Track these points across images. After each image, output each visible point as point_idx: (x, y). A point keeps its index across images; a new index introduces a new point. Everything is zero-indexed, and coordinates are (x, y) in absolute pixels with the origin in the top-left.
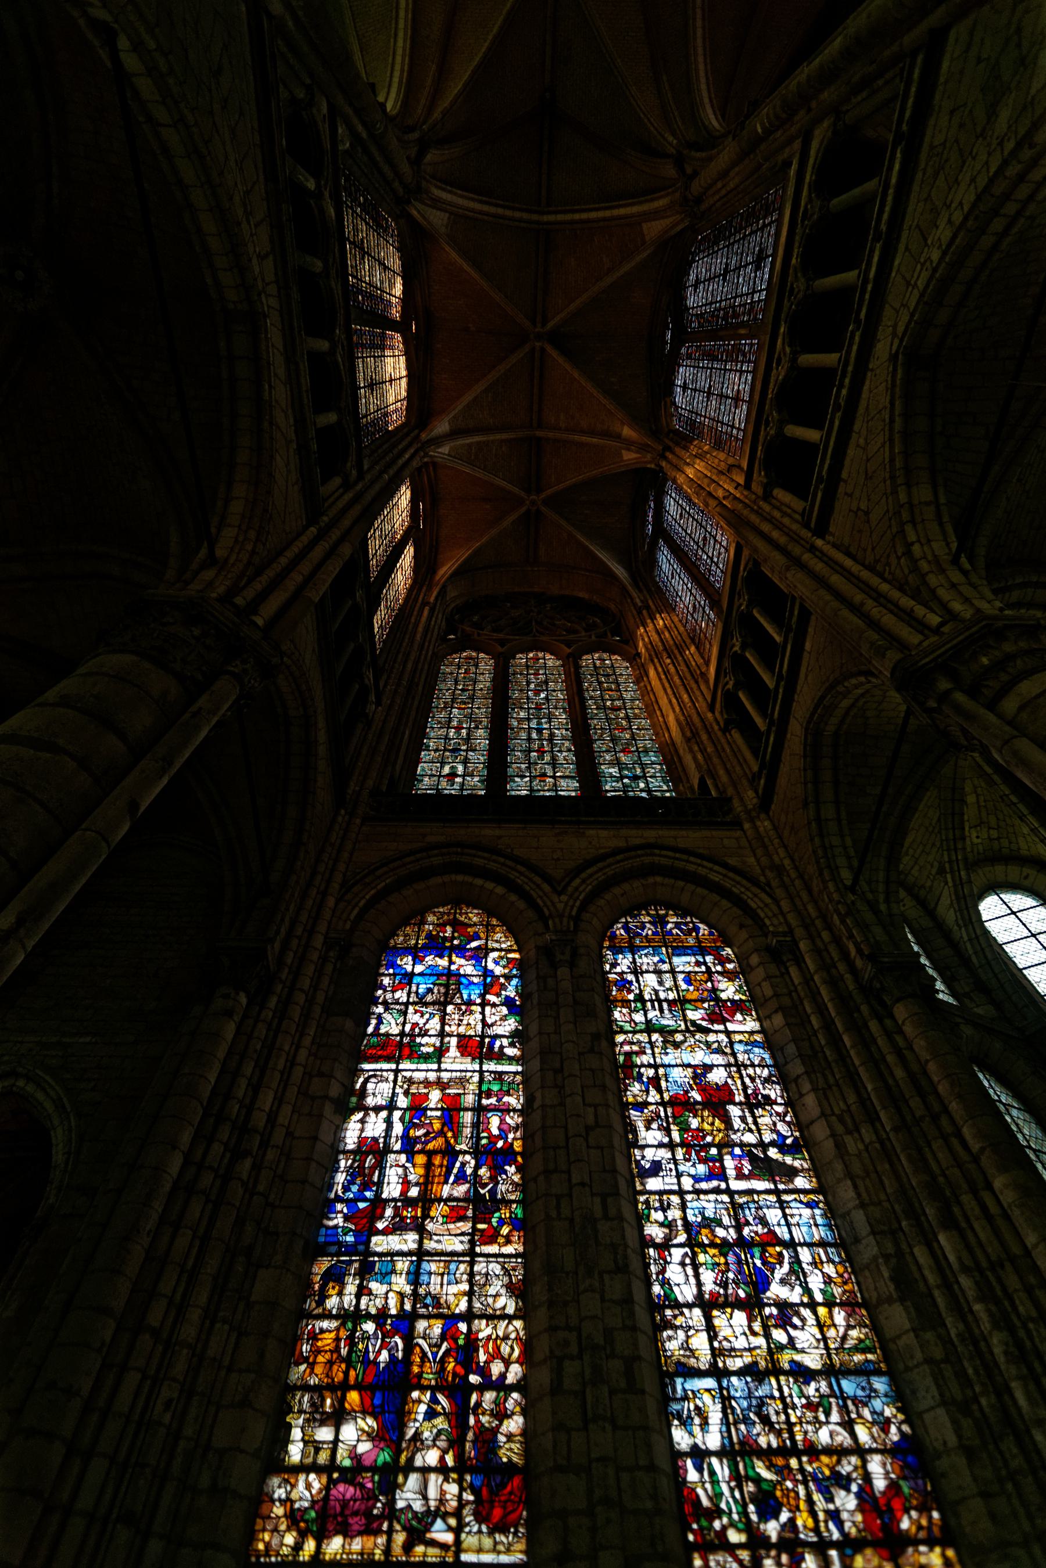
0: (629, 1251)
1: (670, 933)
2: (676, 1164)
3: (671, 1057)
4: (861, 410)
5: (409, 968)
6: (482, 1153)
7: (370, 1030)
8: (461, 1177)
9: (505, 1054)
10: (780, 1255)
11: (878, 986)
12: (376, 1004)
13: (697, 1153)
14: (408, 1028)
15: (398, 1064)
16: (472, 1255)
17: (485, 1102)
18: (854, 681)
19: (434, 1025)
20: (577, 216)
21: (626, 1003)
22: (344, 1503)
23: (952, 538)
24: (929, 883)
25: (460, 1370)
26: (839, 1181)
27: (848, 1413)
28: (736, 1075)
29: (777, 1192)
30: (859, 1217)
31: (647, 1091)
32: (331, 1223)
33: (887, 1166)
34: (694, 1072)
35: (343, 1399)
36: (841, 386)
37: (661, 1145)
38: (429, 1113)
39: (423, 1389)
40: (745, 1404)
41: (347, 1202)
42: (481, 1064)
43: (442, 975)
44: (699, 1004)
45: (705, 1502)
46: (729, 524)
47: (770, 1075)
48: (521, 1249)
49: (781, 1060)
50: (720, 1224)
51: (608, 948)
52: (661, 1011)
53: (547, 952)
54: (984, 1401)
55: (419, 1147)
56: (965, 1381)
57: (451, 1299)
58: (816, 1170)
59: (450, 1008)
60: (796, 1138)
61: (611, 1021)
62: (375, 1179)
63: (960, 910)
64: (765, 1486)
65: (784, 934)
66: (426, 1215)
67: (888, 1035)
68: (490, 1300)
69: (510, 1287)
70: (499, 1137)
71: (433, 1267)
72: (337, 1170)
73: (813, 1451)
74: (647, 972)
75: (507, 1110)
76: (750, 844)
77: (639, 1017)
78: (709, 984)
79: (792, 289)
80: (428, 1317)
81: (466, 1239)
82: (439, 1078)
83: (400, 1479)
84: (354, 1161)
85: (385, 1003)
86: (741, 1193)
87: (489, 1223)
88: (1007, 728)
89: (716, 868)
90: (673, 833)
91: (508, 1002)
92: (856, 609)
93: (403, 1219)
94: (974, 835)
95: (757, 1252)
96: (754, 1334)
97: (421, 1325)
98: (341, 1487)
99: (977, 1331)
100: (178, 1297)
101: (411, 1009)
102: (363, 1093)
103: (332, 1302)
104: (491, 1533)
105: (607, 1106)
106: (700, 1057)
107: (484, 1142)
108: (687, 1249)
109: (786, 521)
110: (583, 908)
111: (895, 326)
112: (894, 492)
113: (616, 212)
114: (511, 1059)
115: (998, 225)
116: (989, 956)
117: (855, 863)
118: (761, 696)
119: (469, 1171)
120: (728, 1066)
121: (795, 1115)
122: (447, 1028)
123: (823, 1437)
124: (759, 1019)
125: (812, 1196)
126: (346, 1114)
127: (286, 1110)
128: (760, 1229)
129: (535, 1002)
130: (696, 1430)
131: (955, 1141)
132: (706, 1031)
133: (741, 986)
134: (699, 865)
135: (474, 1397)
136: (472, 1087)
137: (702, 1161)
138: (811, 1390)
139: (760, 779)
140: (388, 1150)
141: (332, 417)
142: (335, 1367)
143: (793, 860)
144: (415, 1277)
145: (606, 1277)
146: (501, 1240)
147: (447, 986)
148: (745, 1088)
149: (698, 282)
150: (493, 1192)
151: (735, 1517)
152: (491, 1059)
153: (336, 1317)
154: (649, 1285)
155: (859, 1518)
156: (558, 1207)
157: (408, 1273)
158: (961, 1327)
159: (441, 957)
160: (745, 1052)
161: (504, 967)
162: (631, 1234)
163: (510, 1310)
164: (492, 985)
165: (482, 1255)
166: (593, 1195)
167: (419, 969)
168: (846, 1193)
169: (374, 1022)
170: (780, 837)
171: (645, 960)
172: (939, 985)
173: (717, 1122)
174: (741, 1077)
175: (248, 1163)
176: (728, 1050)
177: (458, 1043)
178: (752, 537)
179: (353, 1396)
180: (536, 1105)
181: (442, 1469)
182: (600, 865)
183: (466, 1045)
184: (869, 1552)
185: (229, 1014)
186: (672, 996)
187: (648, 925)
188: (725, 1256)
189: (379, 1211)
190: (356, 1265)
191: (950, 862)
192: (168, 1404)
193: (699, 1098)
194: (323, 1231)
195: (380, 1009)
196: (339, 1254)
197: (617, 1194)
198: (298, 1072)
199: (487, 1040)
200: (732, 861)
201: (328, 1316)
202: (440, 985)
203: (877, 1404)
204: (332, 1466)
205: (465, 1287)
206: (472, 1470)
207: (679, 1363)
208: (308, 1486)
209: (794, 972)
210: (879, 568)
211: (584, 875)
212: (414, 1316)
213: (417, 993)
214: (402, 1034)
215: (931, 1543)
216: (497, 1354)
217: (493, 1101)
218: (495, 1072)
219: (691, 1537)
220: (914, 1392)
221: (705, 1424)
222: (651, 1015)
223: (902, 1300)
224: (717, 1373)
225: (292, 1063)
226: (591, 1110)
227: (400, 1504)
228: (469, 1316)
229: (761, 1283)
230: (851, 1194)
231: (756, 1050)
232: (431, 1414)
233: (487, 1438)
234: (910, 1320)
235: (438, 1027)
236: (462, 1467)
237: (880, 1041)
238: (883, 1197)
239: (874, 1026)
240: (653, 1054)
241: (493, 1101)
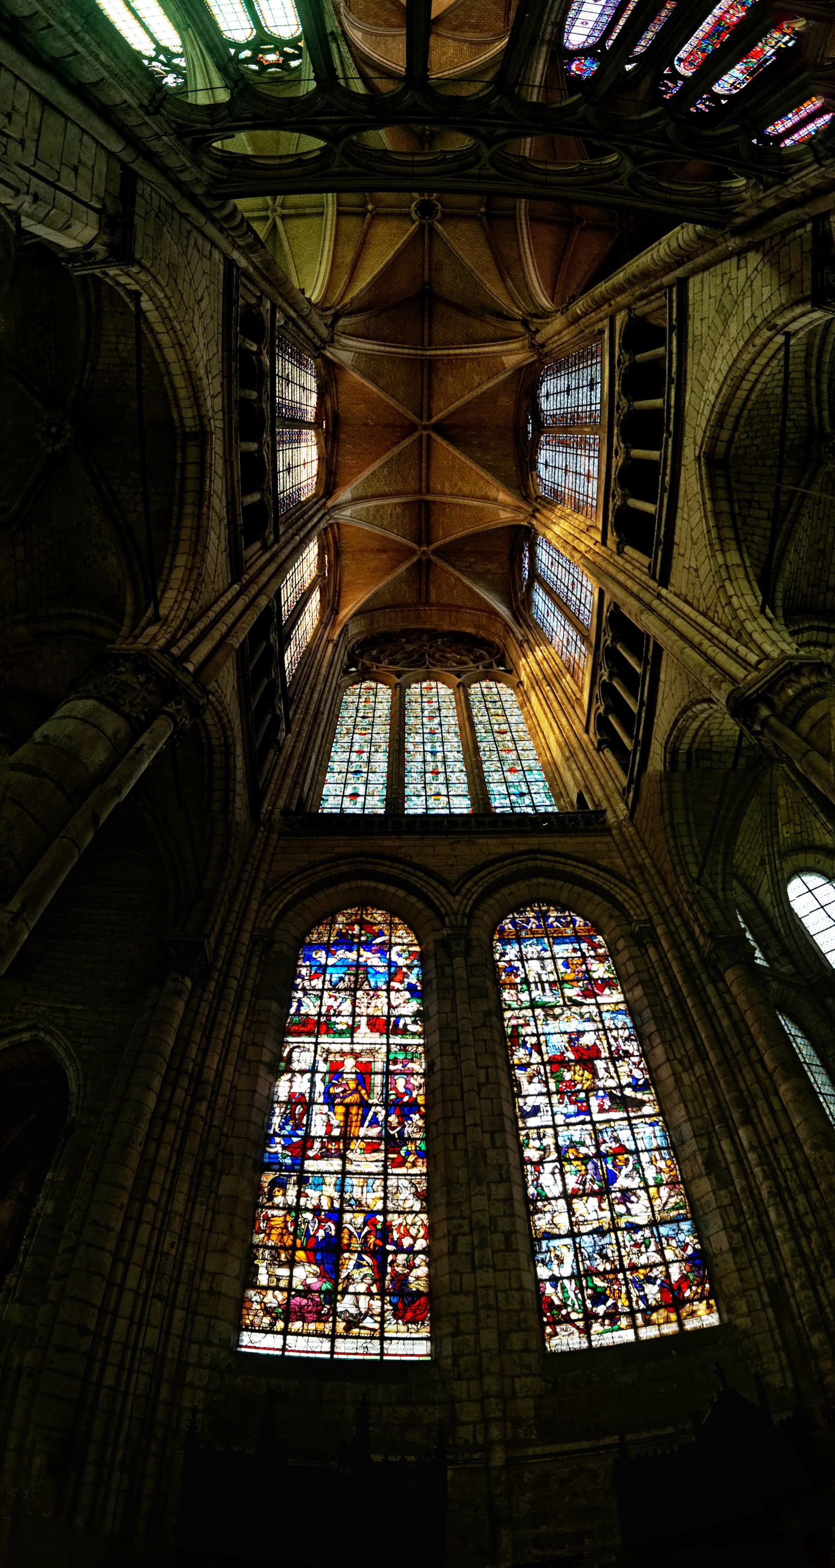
0: (511, 1168)
1: (551, 926)
2: (552, 1106)
3: (553, 1026)
4: (681, 493)
5: (323, 961)
6: (391, 1106)
7: (292, 1011)
8: (374, 1122)
10: (627, 1160)
11: (715, 957)
12: (296, 990)
13: (569, 1097)
14: (324, 1010)
15: (317, 1038)
16: (385, 1174)
17: (392, 1068)
18: (699, 707)
19: (346, 1007)
20: (452, 352)
21: (513, 986)
22: (301, 1307)
23: (759, 593)
24: (753, 874)
25: (379, 1242)
26: (675, 1105)
27: (661, 1244)
28: (603, 1037)
29: (629, 1119)
30: (687, 1129)
31: (530, 1055)
32: (272, 1150)
33: (710, 1090)
34: (570, 1038)
35: (293, 1255)
36: (664, 474)
37: (540, 1094)
38: (345, 1076)
39: (352, 1252)
40: (590, 1250)
41: (283, 1136)
42: (388, 1038)
43: (352, 966)
44: (575, 983)
45: (557, 1302)
46: (592, 574)
47: (630, 1035)
48: (424, 1170)
49: (639, 1023)
50: (583, 1144)
51: (498, 941)
52: (544, 990)
53: (443, 944)
54: (750, 1222)
55: (338, 1100)
56: (740, 1212)
57: (370, 1202)
58: (659, 1101)
59: (359, 994)
60: (646, 1080)
61: (500, 1001)
62: (304, 1121)
63: (775, 893)
64: (599, 1290)
65: (645, 922)
66: (347, 1148)
67: (720, 994)
68: (401, 1203)
69: (417, 1195)
70: (405, 1094)
71: (355, 1181)
72: (273, 1115)
73: (634, 1268)
74: (532, 959)
75: (412, 1074)
76: (617, 846)
77: (524, 997)
78: (584, 967)
79: (618, 406)
80: (353, 1212)
81: (381, 1164)
82: (352, 1049)
83: (339, 1297)
84: (286, 1109)
85: (304, 989)
86: (600, 1122)
87: (399, 1153)
88: (804, 744)
89: (590, 868)
90: (553, 840)
91: (411, 988)
92: (696, 647)
93: (328, 1150)
94: (785, 830)
95: (610, 1160)
96: (602, 1210)
97: (347, 1217)
98: (298, 1299)
99: (753, 1184)
100: (167, 1186)
101: (326, 994)
102: (289, 1060)
103: (279, 1200)
104: (405, 1324)
105: (497, 1067)
106: (575, 1025)
107: (392, 1097)
108: (557, 1164)
109: (637, 573)
110: (475, 907)
111: (695, 438)
112: (714, 556)
113: (481, 350)
114: (413, 1034)
115: (746, 385)
116: (792, 927)
117: (700, 859)
118: (628, 719)
119: (380, 1118)
120: (598, 1030)
121: (647, 1062)
122: (357, 1010)
123: (643, 1260)
124: (623, 992)
125: (655, 1119)
126: (279, 1074)
127: (229, 1071)
128: (614, 1145)
129: (434, 987)
130: (555, 1266)
131: (758, 1066)
132: (581, 1004)
133: (609, 967)
134: (576, 867)
135: (390, 1258)
136: (381, 1056)
137: (572, 1102)
138: (638, 1237)
139: (629, 792)
140: (312, 1102)
141: (256, 497)
142: (285, 1238)
143: (652, 859)
144: (341, 1188)
145: (493, 1186)
146: (408, 1165)
147: (356, 975)
148: (610, 1046)
149: (548, 395)
150: (401, 1133)
151: (577, 1307)
152: (396, 1034)
153: (283, 1209)
154: (526, 1188)
155: (659, 1296)
156: (455, 1142)
157: (335, 1185)
158: (744, 1183)
159: (351, 951)
160: (612, 1019)
161: (406, 959)
162: (513, 1159)
163: (417, 1206)
164: (395, 974)
165: (392, 1174)
166: (483, 1132)
167: (331, 961)
168: (680, 1113)
169: (295, 1004)
170: (642, 841)
171: (530, 949)
172: (758, 954)
173: (586, 1073)
174: (607, 1039)
175: (204, 1105)
176: (598, 1019)
178: (611, 585)
179: (301, 1255)
180: (435, 1069)
181: (369, 1293)
182: (490, 869)
183: (374, 1023)
184: (661, 1311)
185: (179, 994)
186: (553, 978)
187: (532, 920)
188: (586, 1165)
189: (309, 1144)
190: (295, 1178)
191: (769, 855)
192: (172, 1245)
193: (572, 1057)
194: (267, 1155)
195: (300, 994)
196: (280, 1170)
197: (503, 1130)
198: (236, 1041)
199: (392, 1019)
200: (603, 863)
201: (277, 1207)
202: (350, 974)
203: (681, 1237)
204: (289, 1289)
205: (382, 1194)
206: (390, 1294)
207: (545, 1232)
208: (275, 1297)
209: (652, 952)
210: (710, 614)
211: (475, 878)
212: (342, 1211)
213: (330, 981)
214: (319, 1014)
215: (700, 1300)
216: (407, 1233)
217: (399, 1067)
218: (400, 1045)
219: (545, 1319)
220: (707, 1226)
221: (561, 1262)
222: (535, 994)
223: (708, 1174)
224: (571, 1234)
225: (231, 1034)
226: (483, 1072)
227: (339, 1309)
228: (385, 1212)
229: (611, 1178)
230: (683, 1112)
231: (620, 1017)
232: (358, 1266)
233: (401, 1281)
234: (712, 1186)
235: (350, 1009)
236: (382, 1293)
237: (713, 1000)
238: (705, 1111)
239: (710, 989)
240: (536, 1025)
241: (399, 1067)
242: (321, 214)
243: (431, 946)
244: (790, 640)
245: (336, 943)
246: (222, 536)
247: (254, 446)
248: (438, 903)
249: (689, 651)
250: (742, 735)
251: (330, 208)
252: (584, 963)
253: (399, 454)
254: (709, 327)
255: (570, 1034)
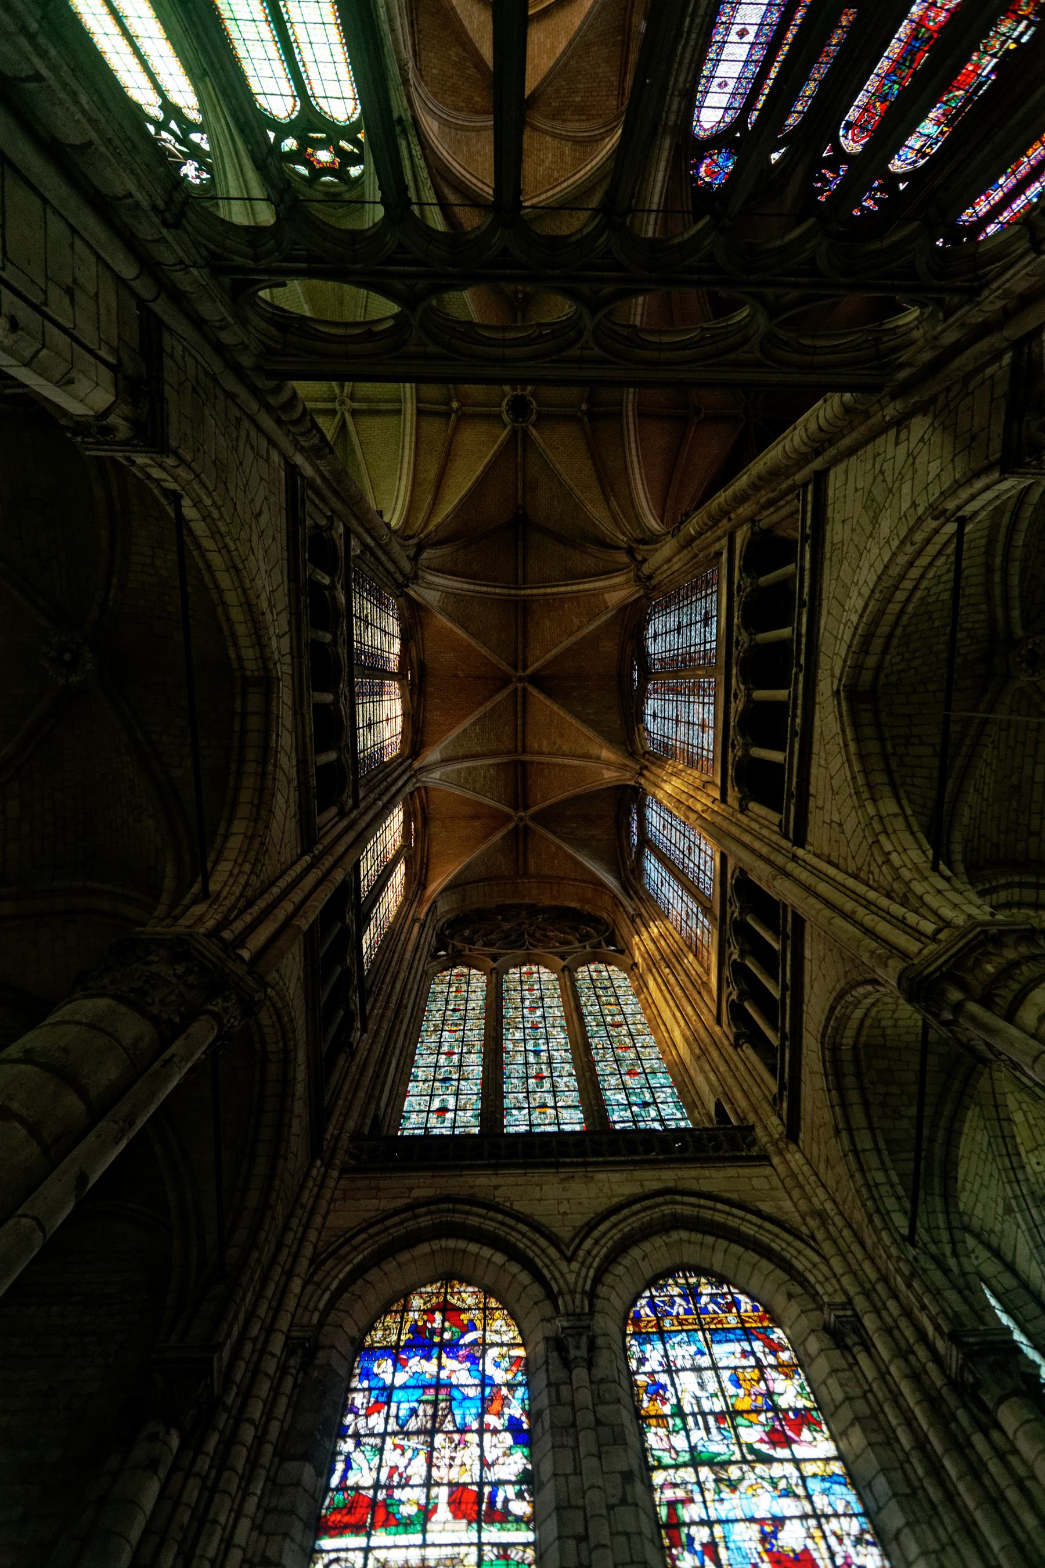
3: (732, 1505)
4: (816, 736)
7: (335, 1481)
9: (509, 1513)
15: (369, 1536)
18: (861, 990)
19: (418, 1470)
20: (549, 590)
28: (817, 1533)
36: (795, 716)
43: (429, 1386)
44: (753, 1417)
46: (711, 835)
51: (634, 1335)
52: (708, 1430)
53: (557, 1344)
59: (439, 1439)
65: (843, 1307)
74: (684, 1369)
77: (680, 1442)
78: (762, 1384)
79: (738, 642)
85: (357, 1436)
90: (694, 1173)
91: (513, 1425)
101: (389, 1442)
106: (766, 1504)
109: (765, 832)
110: (597, 1280)
112: (862, 806)
113: (581, 587)
117: (908, 1206)
118: (769, 1007)
124: (833, 1438)
129: (547, 1424)
139: (781, 1102)
147: (435, 1404)
149: (655, 637)
152: (491, 1522)
159: (428, 1358)
160: (825, 1492)
161: (506, 1370)
170: (816, 1174)
174: (824, 1537)
176: (800, 1491)
177: (450, 1495)
178: (734, 847)
182: (614, 1219)
185: (153, 1465)
186: (718, 1405)
187: (678, 1300)
199: (487, 1490)
200: (766, 1207)
202: (427, 1402)
209: (863, 1359)
210: (863, 875)
211: (596, 1234)
213: (397, 1417)
214: (377, 1486)
222: (697, 1436)
231: (837, 1488)
239: (978, 1441)
242: (398, 412)
243: (541, 1347)
244: (979, 902)
245: (409, 1346)
246: (291, 800)
247: (329, 698)
248: (548, 1276)
249: (839, 921)
250: (926, 1027)
251: (409, 405)
252: (762, 1378)
253: (493, 709)
254: (853, 530)
255: (761, 1522)
